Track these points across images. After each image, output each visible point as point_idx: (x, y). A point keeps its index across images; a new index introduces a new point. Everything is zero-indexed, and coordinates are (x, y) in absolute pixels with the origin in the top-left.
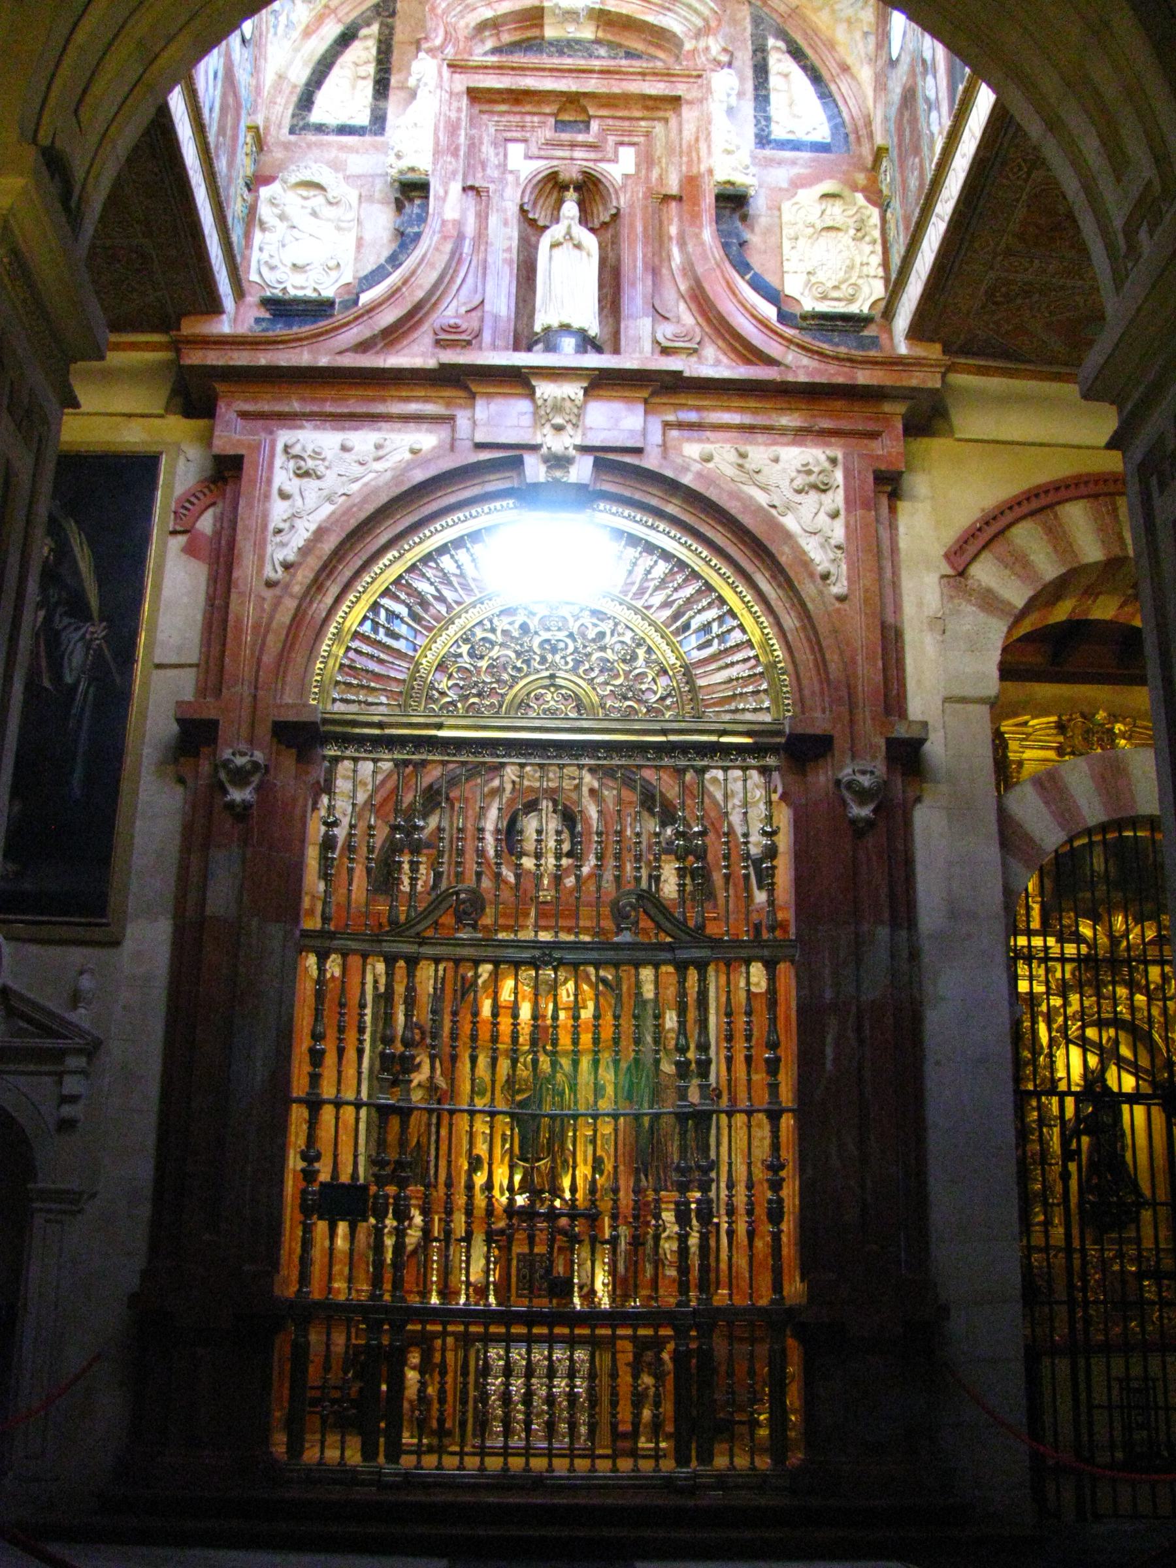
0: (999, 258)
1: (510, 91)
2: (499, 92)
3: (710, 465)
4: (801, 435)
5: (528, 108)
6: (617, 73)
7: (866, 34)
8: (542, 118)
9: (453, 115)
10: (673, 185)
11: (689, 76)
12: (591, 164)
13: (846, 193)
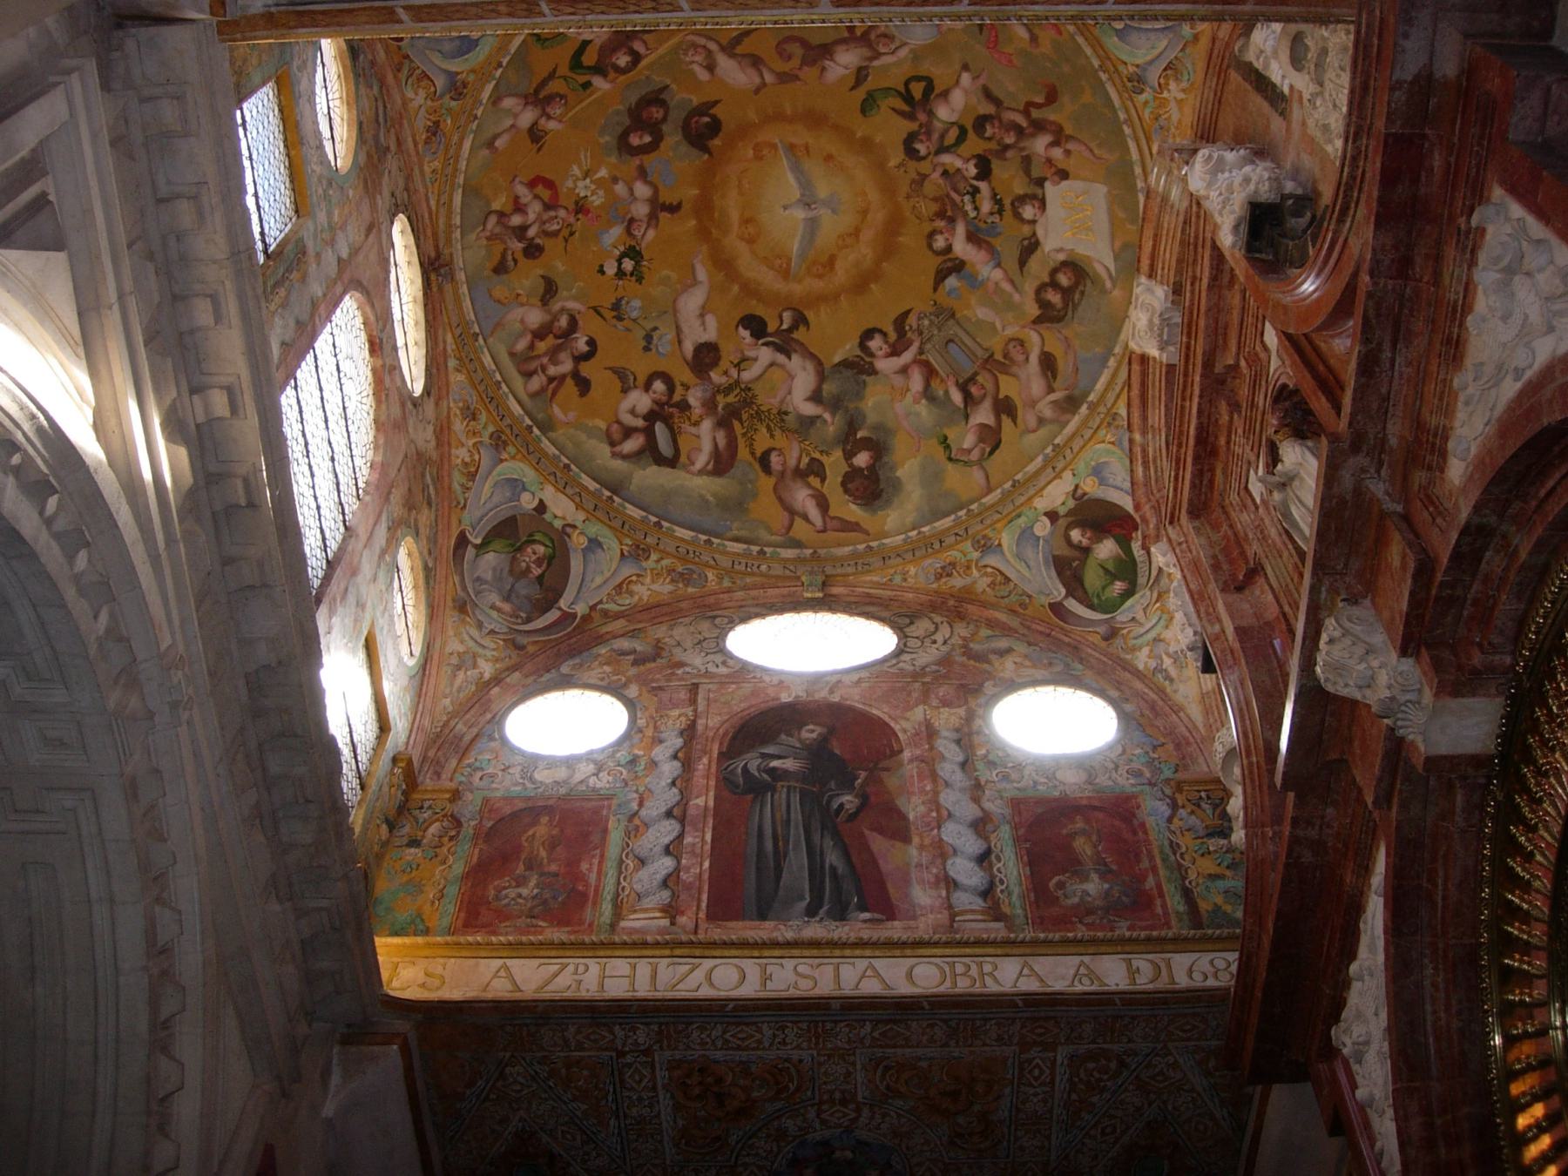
2: (1199, 474)
5: (1222, 441)
6: (1191, 313)
11: (1198, 217)
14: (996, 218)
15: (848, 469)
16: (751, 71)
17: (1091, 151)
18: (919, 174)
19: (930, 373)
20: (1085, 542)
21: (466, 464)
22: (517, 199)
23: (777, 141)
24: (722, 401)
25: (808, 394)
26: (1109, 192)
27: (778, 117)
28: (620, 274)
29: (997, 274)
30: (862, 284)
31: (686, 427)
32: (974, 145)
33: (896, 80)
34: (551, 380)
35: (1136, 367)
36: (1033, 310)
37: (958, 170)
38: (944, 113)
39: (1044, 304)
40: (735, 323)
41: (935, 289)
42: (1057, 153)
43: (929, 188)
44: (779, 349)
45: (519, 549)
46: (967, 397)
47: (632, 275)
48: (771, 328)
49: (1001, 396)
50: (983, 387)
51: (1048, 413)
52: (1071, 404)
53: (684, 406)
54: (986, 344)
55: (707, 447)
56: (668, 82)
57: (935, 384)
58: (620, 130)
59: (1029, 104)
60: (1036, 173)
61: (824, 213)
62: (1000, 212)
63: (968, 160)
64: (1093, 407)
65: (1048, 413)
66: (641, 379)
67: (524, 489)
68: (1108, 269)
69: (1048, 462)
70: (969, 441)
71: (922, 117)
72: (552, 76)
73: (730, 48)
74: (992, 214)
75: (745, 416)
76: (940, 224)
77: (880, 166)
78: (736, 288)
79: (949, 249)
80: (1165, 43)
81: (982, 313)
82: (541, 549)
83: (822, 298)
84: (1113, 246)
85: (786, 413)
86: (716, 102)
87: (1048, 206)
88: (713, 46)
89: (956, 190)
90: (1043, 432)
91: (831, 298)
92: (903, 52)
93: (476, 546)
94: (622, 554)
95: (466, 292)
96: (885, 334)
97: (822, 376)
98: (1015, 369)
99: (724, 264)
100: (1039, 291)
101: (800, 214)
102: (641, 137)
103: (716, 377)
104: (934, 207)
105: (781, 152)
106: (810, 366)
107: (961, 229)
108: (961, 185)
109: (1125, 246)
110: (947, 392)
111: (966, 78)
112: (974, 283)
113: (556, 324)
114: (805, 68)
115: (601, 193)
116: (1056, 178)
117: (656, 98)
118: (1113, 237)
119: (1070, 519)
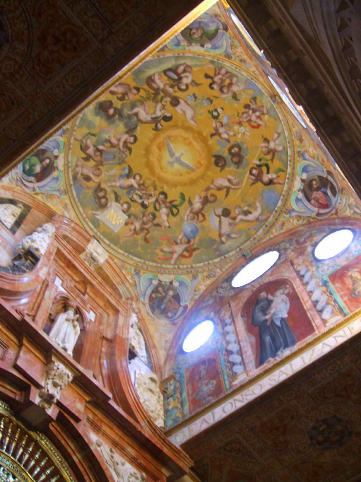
0: (248, 429)
1: (69, 261)
2: (66, 258)
3: (99, 449)
4: (133, 461)
5: (70, 272)
7: (166, 341)
8: (71, 279)
9: (51, 250)
10: (109, 335)
11: (124, 307)
12: (80, 306)
13: (158, 383)
14: (130, 197)
15: (114, 105)
16: (217, 185)
17: (126, 237)
18: (157, 189)
19: (113, 146)
20: (44, 163)
21: (236, 48)
22: (261, 120)
23: (198, 170)
24: (162, 94)
25: (139, 114)
26: (114, 233)
27: (203, 177)
28: (216, 110)
29: (118, 184)
30: (148, 150)
31: (168, 82)
32: (151, 209)
33: (181, 208)
34: (219, 74)
35: (88, 237)
36: (103, 186)
37: (149, 199)
38: (164, 210)
39: (102, 190)
40: (173, 115)
41: (129, 166)
42: (132, 227)
43: (151, 188)
44: (157, 118)
45: (202, 35)
46: (98, 150)
47: (212, 112)
48: (162, 122)
49: (91, 160)
50: (97, 156)
51: (77, 169)
52: (75, 178)
53: (172, 86)
54: (105, 166)
55: (157, 81)
56: (238, 170)
57: (109, 145)
58: (242, 150)
59: (148, 232)
60: (132, 217)
61: (171, 160)
62: (131, 200)
63: (149, 204)
64: (71, 186)
65: (77, 169)
66: (190, 87)
67: (212, 48)
68: (97, 215)
69: (68, 162)
70: (89, 142)
71: (168, 204)
72: (272, 160)
73: (228, 189)
74: (132, 197)
75: (152, 95)
76: (141, 182)
77: (167, 183)
78: (180, 124)
79: (134, 178)
80: (142, 290)
81: (113, 172)
82: (195, 36)
83: (155, 137)
84: (102, 222)
85: (141, 104)
86: (221, 171)
87: (123, 213)
88: (233, 187)
89: (146, 194)
90: (74, 164)
91: (152, 140)
92: (186, 218)
93: (219, 29)
94: (167, 47)
95: (262, 90)
96: (132, 143)
97: (139, 120)
98: (94, 168)
99: (188, 129)
100: (106, 191)
101: (177, 155)
102: (235, 151)
103: (169, 99)
104: (146, 185)
105: (194, 168)
106: (144, 120)
107: (136, 185)
108: (145, 196)
109: (99, 225)
110: (104, 145)
111: (167, 224)
112: (121, 176)
113: (227, 88)
114: (205, 195)
115: (236, 130)
116: (127, 221)
117: (238, 164)
118: (103, 223)
119: (52, 162)
